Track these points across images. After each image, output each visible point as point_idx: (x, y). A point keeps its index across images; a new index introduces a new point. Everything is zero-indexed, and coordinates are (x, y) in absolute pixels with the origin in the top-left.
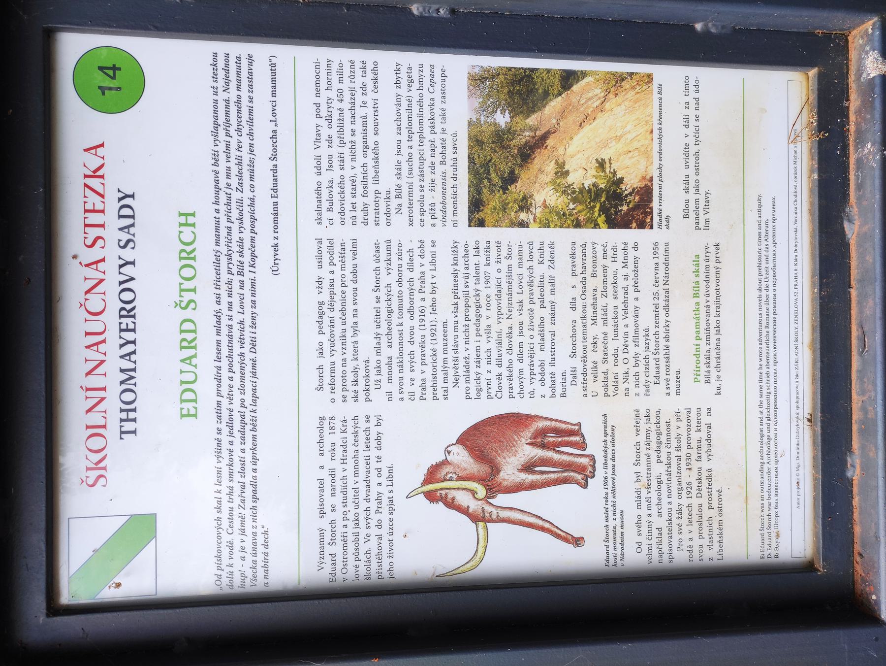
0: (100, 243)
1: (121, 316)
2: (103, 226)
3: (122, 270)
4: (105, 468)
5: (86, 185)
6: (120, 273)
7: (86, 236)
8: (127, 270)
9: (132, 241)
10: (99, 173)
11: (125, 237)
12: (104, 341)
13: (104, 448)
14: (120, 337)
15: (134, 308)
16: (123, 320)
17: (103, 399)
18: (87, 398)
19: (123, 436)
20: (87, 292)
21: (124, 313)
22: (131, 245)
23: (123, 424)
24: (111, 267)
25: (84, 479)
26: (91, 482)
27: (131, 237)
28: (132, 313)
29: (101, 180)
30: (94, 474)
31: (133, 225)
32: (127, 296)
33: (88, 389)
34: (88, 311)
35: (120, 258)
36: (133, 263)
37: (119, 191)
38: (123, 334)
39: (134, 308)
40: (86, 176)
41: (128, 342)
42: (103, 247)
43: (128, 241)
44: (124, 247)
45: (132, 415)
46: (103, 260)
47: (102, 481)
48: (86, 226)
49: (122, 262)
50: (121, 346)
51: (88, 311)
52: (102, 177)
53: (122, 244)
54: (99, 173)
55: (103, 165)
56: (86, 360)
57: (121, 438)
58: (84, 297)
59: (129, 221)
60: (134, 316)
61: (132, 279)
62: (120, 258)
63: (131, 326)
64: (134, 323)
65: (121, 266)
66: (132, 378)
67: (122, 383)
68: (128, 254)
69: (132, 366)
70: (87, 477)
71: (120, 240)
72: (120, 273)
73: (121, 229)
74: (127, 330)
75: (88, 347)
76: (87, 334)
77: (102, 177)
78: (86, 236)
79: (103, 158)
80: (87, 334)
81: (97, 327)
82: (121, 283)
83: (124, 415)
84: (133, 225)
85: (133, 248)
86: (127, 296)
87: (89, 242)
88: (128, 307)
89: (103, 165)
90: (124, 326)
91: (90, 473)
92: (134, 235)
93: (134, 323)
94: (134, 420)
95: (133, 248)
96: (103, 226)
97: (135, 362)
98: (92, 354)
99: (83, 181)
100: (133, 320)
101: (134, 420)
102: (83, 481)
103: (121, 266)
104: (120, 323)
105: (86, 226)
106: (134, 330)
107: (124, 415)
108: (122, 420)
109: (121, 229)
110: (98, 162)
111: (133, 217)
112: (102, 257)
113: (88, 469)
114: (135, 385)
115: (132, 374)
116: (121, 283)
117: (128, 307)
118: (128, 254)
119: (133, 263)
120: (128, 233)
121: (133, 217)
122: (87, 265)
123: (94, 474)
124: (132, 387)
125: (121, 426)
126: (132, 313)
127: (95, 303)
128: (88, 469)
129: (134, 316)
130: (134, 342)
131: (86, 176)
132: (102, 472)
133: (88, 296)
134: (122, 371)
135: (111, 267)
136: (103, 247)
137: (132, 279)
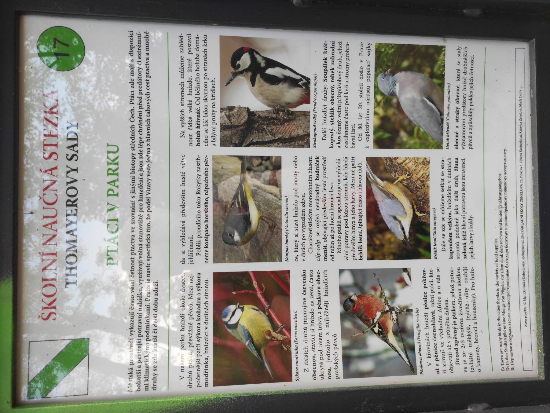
0: (54, 156)
1: (68, 206)
2: (56, 145)
3: (68, 175)
4: (55, 308)
6: (67, 177)
8: (72, 174)
9: (76, 155)
11: (71, 153)
12: (55, 222)
13: (55, 294)
14: (67, 220)
15: (77, 200)
16: (69, 208)
20: (46, 189)
21: (70, 203)
22: (75, 158)
24: (61, 172)
26: (45, 316)
27: (75, 153)
28: (75, 203)
30: (47, 312)
31: (76, 145)
32: (72, 192)
33: (43, 254)
34: (44, 201)
35: (67, 167)
36: (76, 170)
39: (77, 200)
41: (72, 223)
42: (56, 160)
44: (71, 159)
45: (73, 272)
46: (56, 168)
47: (53, 316)
48: (45, 145)
49: (69, 169)
50: (67, 225)
51: (44, 201)
53: (69, 157)
54: (54, 110)
58: (42, 193)
60: (76, 206)
61: (76, 180)
62: (67, 167)
64: (77, 210)
65: (68, 172)
66: (74, 246)
68: (73, 164)
69: (73, 238)
70: (43, 314)
71: (67, 155)
72: (67, 177)
73: (69, 147)
75: (45, 226)
76: (45, 217)
80: (45, 217)
81: (51, 213)
82: (68, 183)
83: (68, 271)
84: (76, 145)
85: (76, 160)
86: (72, 192)
88: (73, 199)
92: (77, 152)
93: (77, 210)
94: (75, 275)
95: (76, 160)
96: (56, 145)
97: (76, 236)
98: (47, 231)
100: (75, 208)
101: (75, 275)
102: (39, 317)
103: (68, 172)
104: (67, 210)
105: (45, 145)
109: (69, 147)
111: (77, 139)
112: (54, 166)
114: (76, 251)
115: (75, 244)
116: (68, 183)
117: (73, 199)
118: (73, 164)
119: (76, 170)
120: (73, 150)
121: (77, 139)
122: (46, 171)
123: (47, 312)
124: (75, 253)
126: (75, 203)
127: (50, 197)
129: (76, 206)
132: (53, 310)
133: (46, 192)
134: (67, 242)
135: (61, 172)
136: (56, 160)
137: (76, 180)
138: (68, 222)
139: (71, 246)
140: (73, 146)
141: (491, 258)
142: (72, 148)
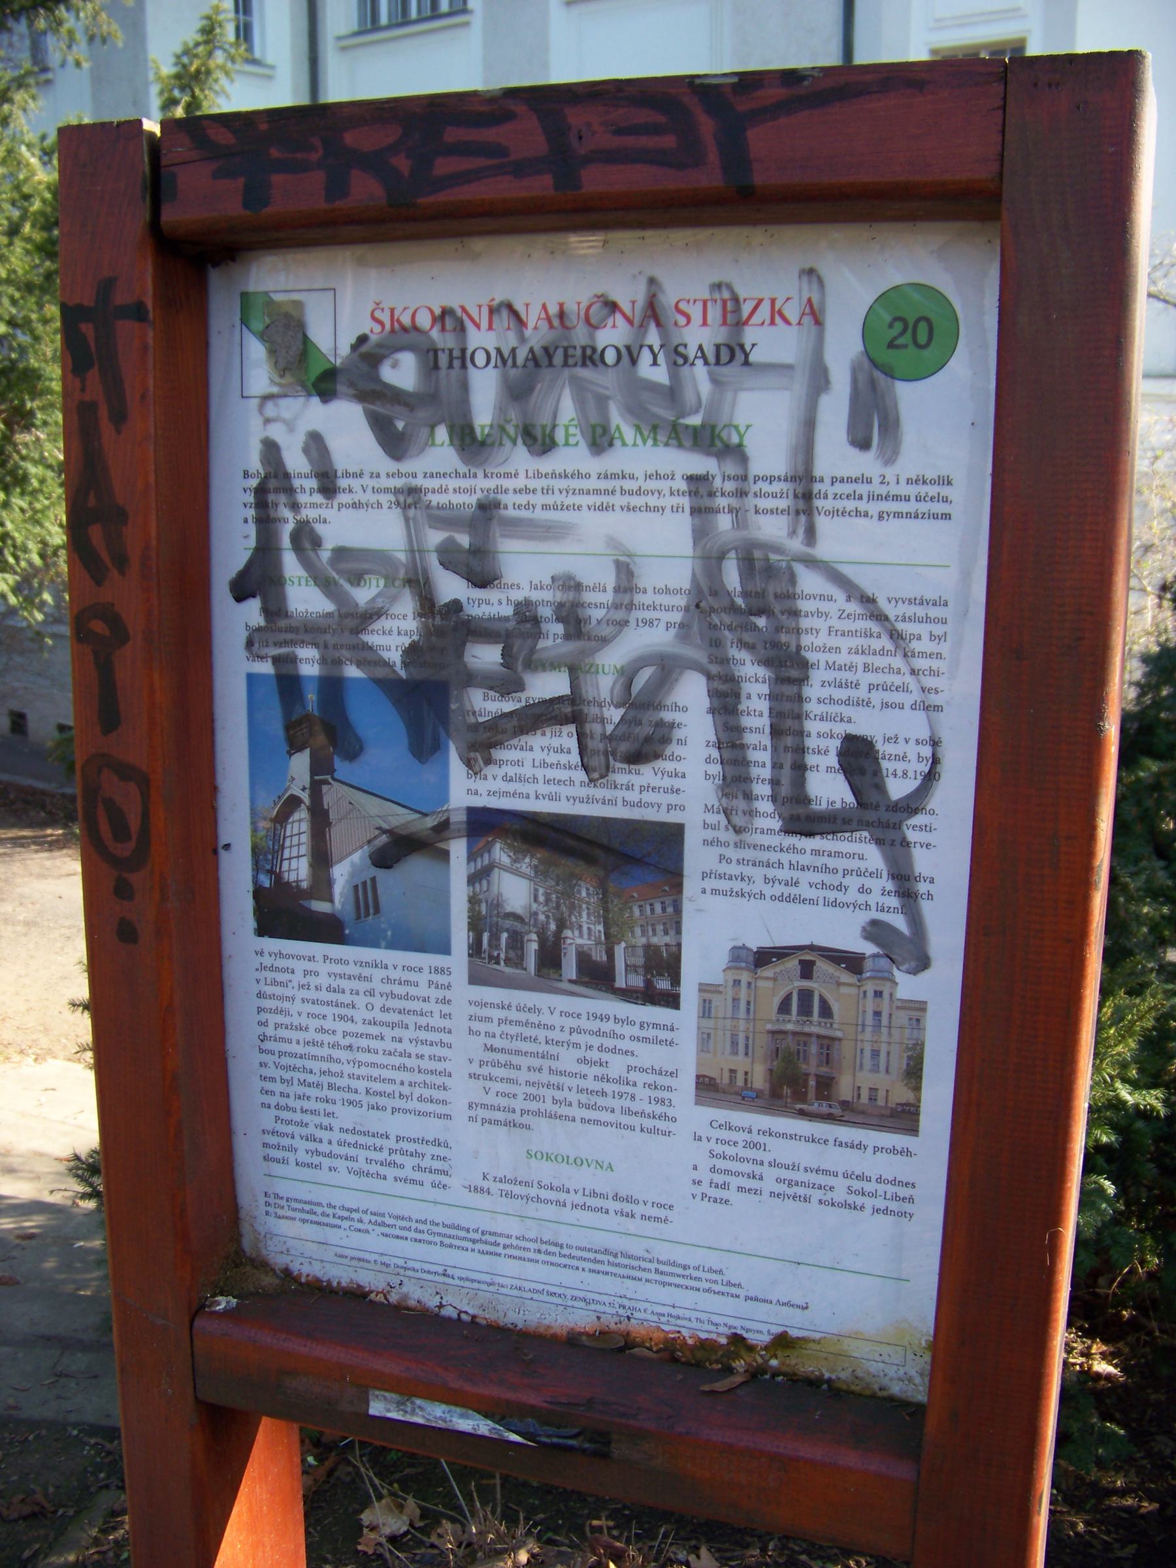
2: (705, 323)
5: (760, 301)
7: (692, 302)
9: (685, 363)
10: (778, 319)
16: (579, 352)
17: (478, 326)
18: (480, 307)
19: (431, 354)
21: (589, 352)
23: (447, 352)
25: (381, 306)
26: (378, 314)
28: (588, 363)
29: (768, 321)
37: (753, 345)
38: (560, 352)
39: (594, 364)
40: (773, 301)
43: (685, 358)
52: (773, 323)
54: (778, 319)
55: (787, 322)
56: (527, 305)
57: (428, 351)
59: (711, 358)
63: (571, 361)
67: (499, 351)
73: (700, 348)
74: (566, 356)
77: (773, 323)
78: (692, 302)
79: (799, 324)
87: (682, 306)
89: (787, 322)
90: (571, 352)
91: (387, 313)
93: (575, 365)
99: (766, 295)
105: (705, 303)
106: (565, 364)
107: (456, 353)
108: (451, 351)
109: (700, 348)
110: (793, 317)
113: (392, 311)
115: (510, 362)
117: (597, 357)
120: (696, 357)
124: (493, 363)
125: (443, 350)
128: (392, 311)
129: (584, 365)
130: (551, 365)
131: (773, 301)
134: (513, 350)
138: (551, 351)
139: (506, 356)
140: (704, 357)
141: (465, 1218)
142: (699, 354)
